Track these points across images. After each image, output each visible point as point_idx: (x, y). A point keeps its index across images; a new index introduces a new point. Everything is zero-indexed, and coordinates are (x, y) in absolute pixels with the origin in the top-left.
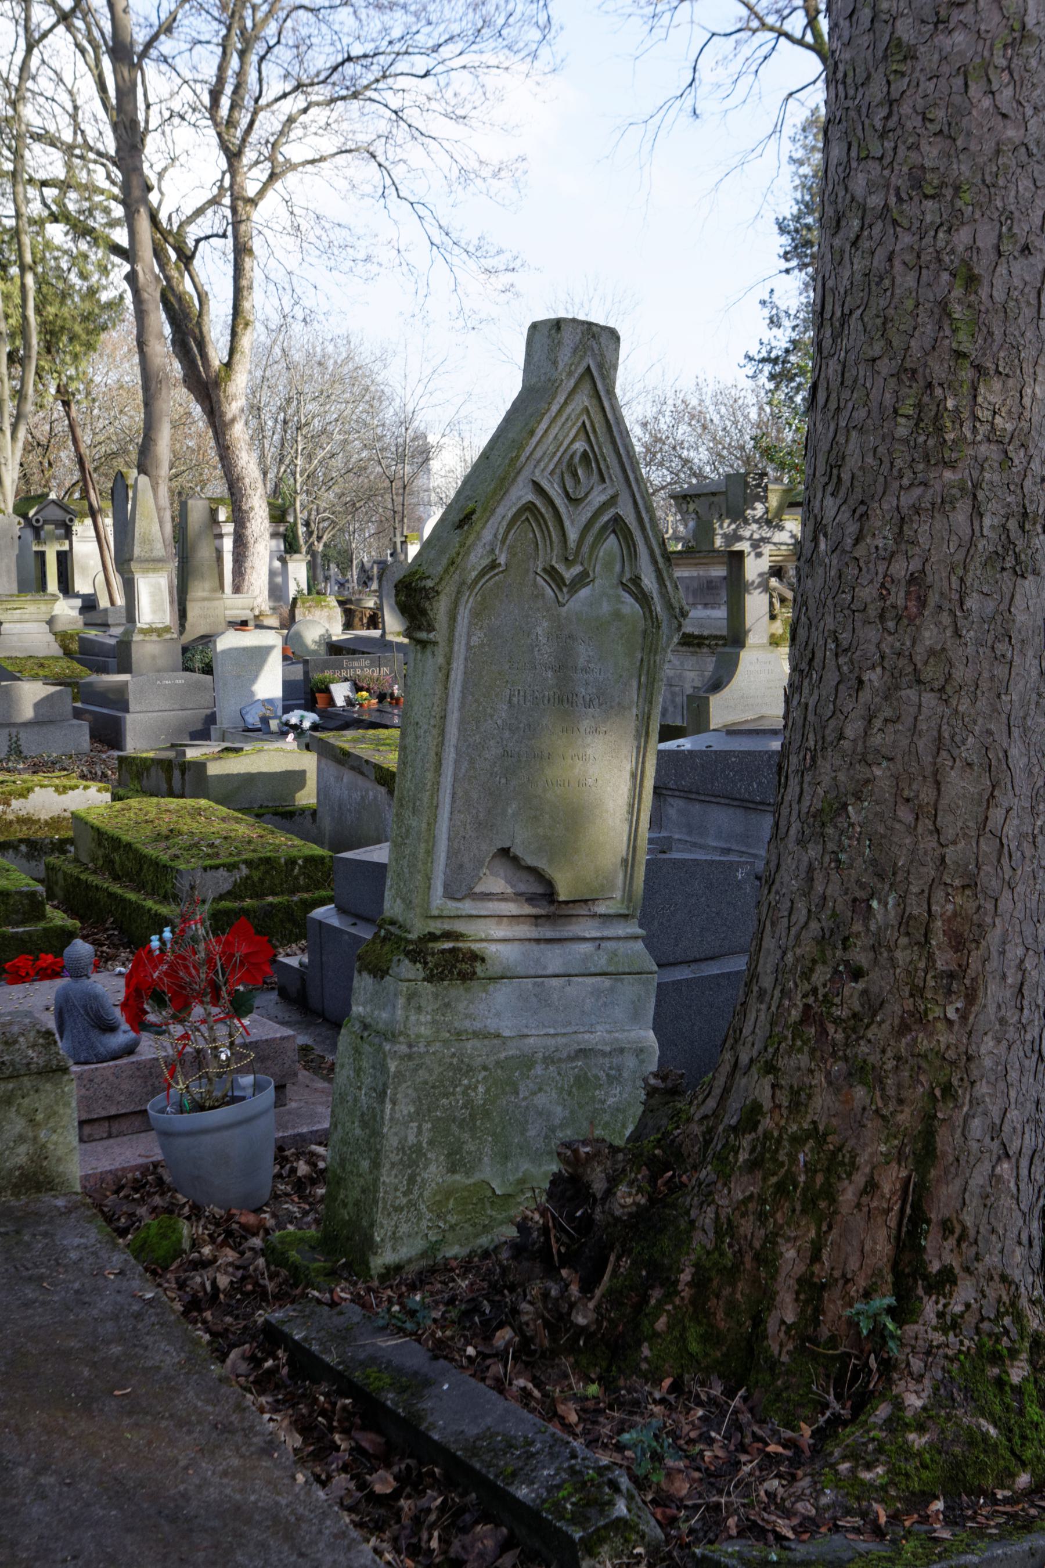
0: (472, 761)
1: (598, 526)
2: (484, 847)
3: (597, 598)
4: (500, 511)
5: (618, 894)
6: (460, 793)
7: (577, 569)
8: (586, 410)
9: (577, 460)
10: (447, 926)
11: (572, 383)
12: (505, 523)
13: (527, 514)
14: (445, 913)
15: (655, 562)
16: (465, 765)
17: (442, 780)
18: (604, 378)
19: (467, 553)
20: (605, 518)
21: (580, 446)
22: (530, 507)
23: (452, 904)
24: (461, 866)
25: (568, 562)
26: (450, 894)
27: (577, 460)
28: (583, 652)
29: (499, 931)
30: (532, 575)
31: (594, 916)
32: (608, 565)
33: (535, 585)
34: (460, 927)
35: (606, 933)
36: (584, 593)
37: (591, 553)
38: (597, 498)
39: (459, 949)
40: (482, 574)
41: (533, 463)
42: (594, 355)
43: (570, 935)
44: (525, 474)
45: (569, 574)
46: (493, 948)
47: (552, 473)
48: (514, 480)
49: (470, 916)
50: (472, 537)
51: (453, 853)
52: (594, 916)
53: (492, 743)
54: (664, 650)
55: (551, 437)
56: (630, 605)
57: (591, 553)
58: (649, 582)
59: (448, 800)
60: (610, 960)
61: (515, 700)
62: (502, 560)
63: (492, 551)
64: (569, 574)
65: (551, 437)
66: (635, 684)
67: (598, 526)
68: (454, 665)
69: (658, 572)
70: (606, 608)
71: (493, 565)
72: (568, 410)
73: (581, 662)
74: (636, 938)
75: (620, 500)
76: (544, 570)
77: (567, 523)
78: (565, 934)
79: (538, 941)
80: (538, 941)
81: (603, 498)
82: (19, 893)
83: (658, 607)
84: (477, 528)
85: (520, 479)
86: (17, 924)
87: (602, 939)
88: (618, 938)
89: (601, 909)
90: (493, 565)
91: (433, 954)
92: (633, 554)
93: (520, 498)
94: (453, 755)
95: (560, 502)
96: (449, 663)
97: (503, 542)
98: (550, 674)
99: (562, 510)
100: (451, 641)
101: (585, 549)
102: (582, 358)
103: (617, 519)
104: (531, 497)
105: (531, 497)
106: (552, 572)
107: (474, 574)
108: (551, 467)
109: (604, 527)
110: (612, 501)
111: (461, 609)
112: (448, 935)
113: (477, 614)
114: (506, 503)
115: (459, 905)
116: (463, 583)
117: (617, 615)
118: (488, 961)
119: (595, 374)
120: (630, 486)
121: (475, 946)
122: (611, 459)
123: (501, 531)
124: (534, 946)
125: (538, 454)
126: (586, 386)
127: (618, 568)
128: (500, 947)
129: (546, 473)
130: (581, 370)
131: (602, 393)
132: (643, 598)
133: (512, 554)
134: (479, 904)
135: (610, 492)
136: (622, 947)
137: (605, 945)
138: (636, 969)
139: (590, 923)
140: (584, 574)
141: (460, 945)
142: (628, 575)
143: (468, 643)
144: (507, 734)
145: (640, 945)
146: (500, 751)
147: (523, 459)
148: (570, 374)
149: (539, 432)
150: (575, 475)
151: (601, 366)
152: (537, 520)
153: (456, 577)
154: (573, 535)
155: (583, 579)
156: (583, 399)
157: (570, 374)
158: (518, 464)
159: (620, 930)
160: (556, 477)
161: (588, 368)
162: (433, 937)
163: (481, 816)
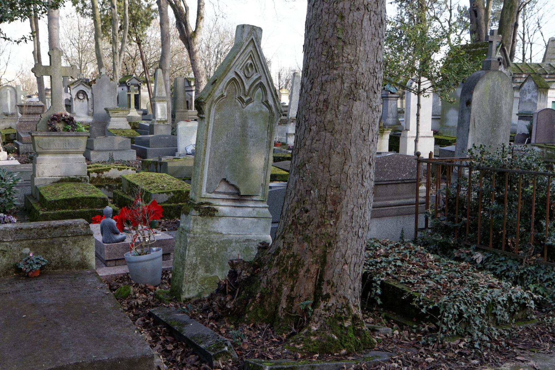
0: (215, 153)
1: (255, 85)
3: (255, 106)
4: (225, 80)
5: (260, 194)
6: (211, 162)
7: (248, 98)
8: (251, 51)
9: (248, 65)
10: (207, 201)
11: (247, 43)
15: (273, 96)
16: (213, 154)
18: (257, 42)
19: (214, 92)
20: (257, 83)
21: (250, 62)
22: (234, 79)
25: (246, 96)
26: (208, 191)
27: (248, 65)
28: (250, 122)
31: (253, 200)
32: (258, 97)
36: (251, 105)
37: (253, 93)
38: (255, 77)
40: (219, 98)
44: (233, 69)
45: (245, 99)
46: (220, 208)
47: (241, 69)
48: (229, 71)
51: (209, 179)
52: (253, 200)
54: (276, 123)
56: (265, 109)
57: (253, 93)
58: (271, 102)
59: (208, 164)
60: (257, 214)
62: (225, 94)
64: (245, 99)
65: (241, 58)
66: (266, 132)
67: (255, 85)
68: (210, 124)
69: (274, 99)
70: (257, 109)
73: (249, 125)
74: (266, 207)
75: (262, 78)
77: (245, 84)
78: (243, 205)
79: (235, 206)
80: (235, 206)
81: (257, 77)
82: (100, 198)
83: (274, 110)
84: (217, 85)
85: (231, 71)
86: (99, 208)
88: (260, 207)
89: (255, 198)
90: (222, 96)
92: (266, 94)
94: (209, 151)
95: (243, 78)
96: (208, 124)
97: (226, 89)
98: (239, 128)
99: (244, 80)
100: (209, 117)
101: (251, 92)
102: (250, 36)
103: (261, 83)
104: (234, 76)
105: (234, 76)
106: (240, 98)
107: (216, 98)
109: (257, 85)
110: (260, 78)
111: (212, 108)
112: (207, 203)
113: (217, 110)
115: (211, 195)
116: (213, 101)
117: (261, 112)
120: (265, 74)
121: (215, 207)
122: (259, 66)
125: (237, 63)
126: (252, 45)
127: (261, 98)
130: (250, 39)
131: (257, 47)
132: (269, 107)
134: (217, 195)
135: (259, 75)
136: (261, 210)
137: (255, 209)
139: (251, 202)
140: (250, 99)
142: (264, 100)
144: (226, 145)
145: (267, 210)
147: (232, 65)
148: (247, 40)
149: (237, 58)
150: (248, 70)
151: (256, 38)
153: (211, 99)
154: (247, 88)
155: (250, 101)
156: (251, 48)
157: (247, 40)
159: (261, 205)
162: (202, 204)
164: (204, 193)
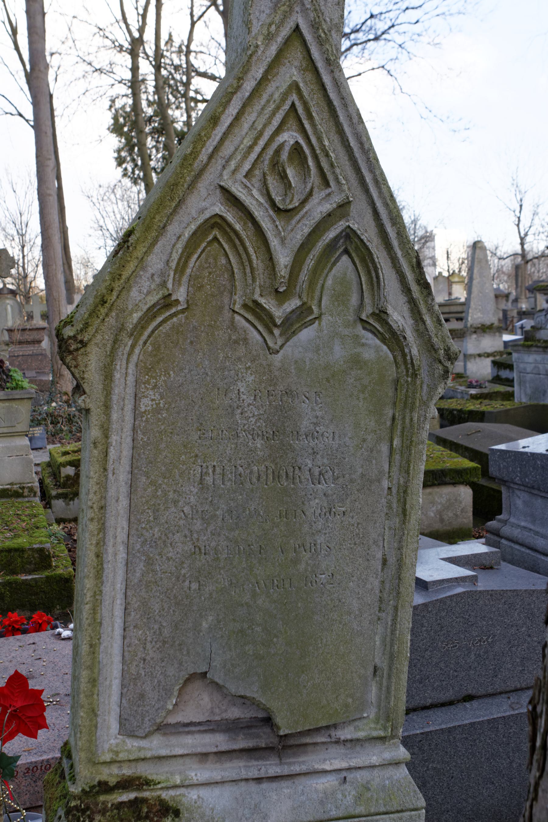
0: (149, 562)
1: (320, 245)
2: (171, 671)
3: (328, 339)
4: (173, 229)
5: (371, 713)
6: (135, 603)
7: (293, 303)
8: (295, 87)
9: (284, 156)
10: (127, 771)
11: (273, 50)
12: (180, 246)
13: (216, 232)
14: (122, 756)
15: (407, 290)
16: (140, 567)
17: (107, 589)
18: (321, 42)
19: (126, 288)
20: (331, 234)
21: (289, 137)
22: (217, 222)
23: (132, 743)
24: (142, 696)
25: (281, 296)
26: (127, 729)
27: (284, 156)
28: (307, 413)
29: (198, 773)
30: (227, 314)
31: (338, 742)
32: (340, 298)
33: (233, 325)
34: (144, 770)
35: (353, 763)
36: (306, 334)
37: (312, 283)
38: (319, 207)
39: (144, 801)
40: (151, 313)
41: (220, 162)
42: (304, 10)
43: (304, 768)
44: (209, 178)
45: (279, 313)
46: (193, 794)
47: (248, 175)
48: (192, 186)
49: (160, 758)
50: (131, 266)
51: (128, 680)
52: (338, 742)
53: (177, 537)
54: (425, 404)
55: (246, 126)
56: (373, 348)
57: (312, 283)
58: (399, 316)
59: (118, 612)
60: (358, 798)
61: (209, 480)
62: (181, 295)
63: (164, 284)
64: (279, 313)
65: (246, 126)
66: (385, 448)
67: (320, 245)
68: (114, 438)
69: (412, 302)
70: (339, 353)
71: (167, 302)
72: (271, 88)
73: (305, 425)
74: (397, 764)
75: (353, 210)
76: (245, 306)
77: (274, 242)
78: (296, 769)
79: (259, 780)
80: (259, 780)
81: (327, 207)
82: (32, 549)
83: (414, 349)
84: (139, 253)
85: (203, 186)
86: (30, 573)
87: (349, 769)
88: (373, 767)
89: (346, 733)
90: (167, 302)
91: (103, 812)
92: (375, 283)
93: (202, 211)
94: (122, 555)
95: (262, 215)
96: (107, 436)
97: (181, 269)
98: (259, 443)
99: (266, 225)
100: (107, 407)
101: (304, 276)
102: (286, 16)
103: (349, 235)
104: (219, 208)
105: (219, 208)
106: (255, 308)
107: (136, 316)
108: (247, 166)
109: (332, 246)
110: (343, 208)
111: (120, 365)
112: (125, 784)
113: (146, 370)
114: (182, 216)
115: (143, 743)
116: (122, 329)
117: (356, 361)
118: (185, 815)
119: (308, 37)
120: (367, 191)
121: (165, 795)
122: (337, 153)
123: (175, 256)
124: (253, 787)
125: (228, 149)
126: (296, 55)
127: (354, 300)
128: (204, 792)
129: (240, 176)
130: (285, 31)
131: (320, 65)
132: (393, 339)
133: (196, 285)
134: (174, 740)
135: (337, 199)
136: (377, 778)
137: (350, 776)
138: (396, 807)
139: (334, 750)
140: (304, 310)
141: (146, 794)
142: (369, 309)
143: (135, 408)
144: (198, 525)
145: (404, 771)
146: (189, 547)
147: (203, 157)
148: (269, 37)
149: (226, 121)
150: (283, 177)
151: (315, 26)
152: (230, 240)
153: (111, 320)
154: (283, 259)
155: (302, 317)
156: (291, 72)
157: (269, 37)
158: (197, 165)
159: (374, 756)
160: (256, 181)
161: (297, 28)
162: (104, 787)
163: (166, 632)
164: (109, 736)
